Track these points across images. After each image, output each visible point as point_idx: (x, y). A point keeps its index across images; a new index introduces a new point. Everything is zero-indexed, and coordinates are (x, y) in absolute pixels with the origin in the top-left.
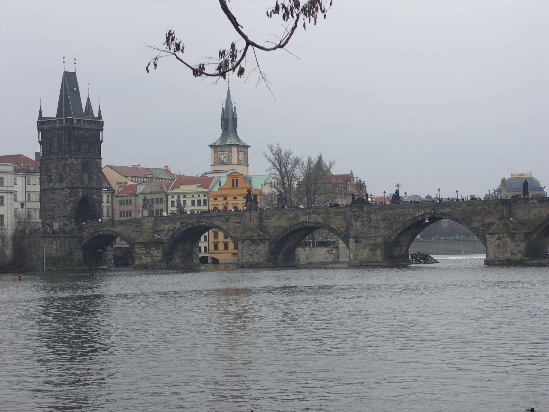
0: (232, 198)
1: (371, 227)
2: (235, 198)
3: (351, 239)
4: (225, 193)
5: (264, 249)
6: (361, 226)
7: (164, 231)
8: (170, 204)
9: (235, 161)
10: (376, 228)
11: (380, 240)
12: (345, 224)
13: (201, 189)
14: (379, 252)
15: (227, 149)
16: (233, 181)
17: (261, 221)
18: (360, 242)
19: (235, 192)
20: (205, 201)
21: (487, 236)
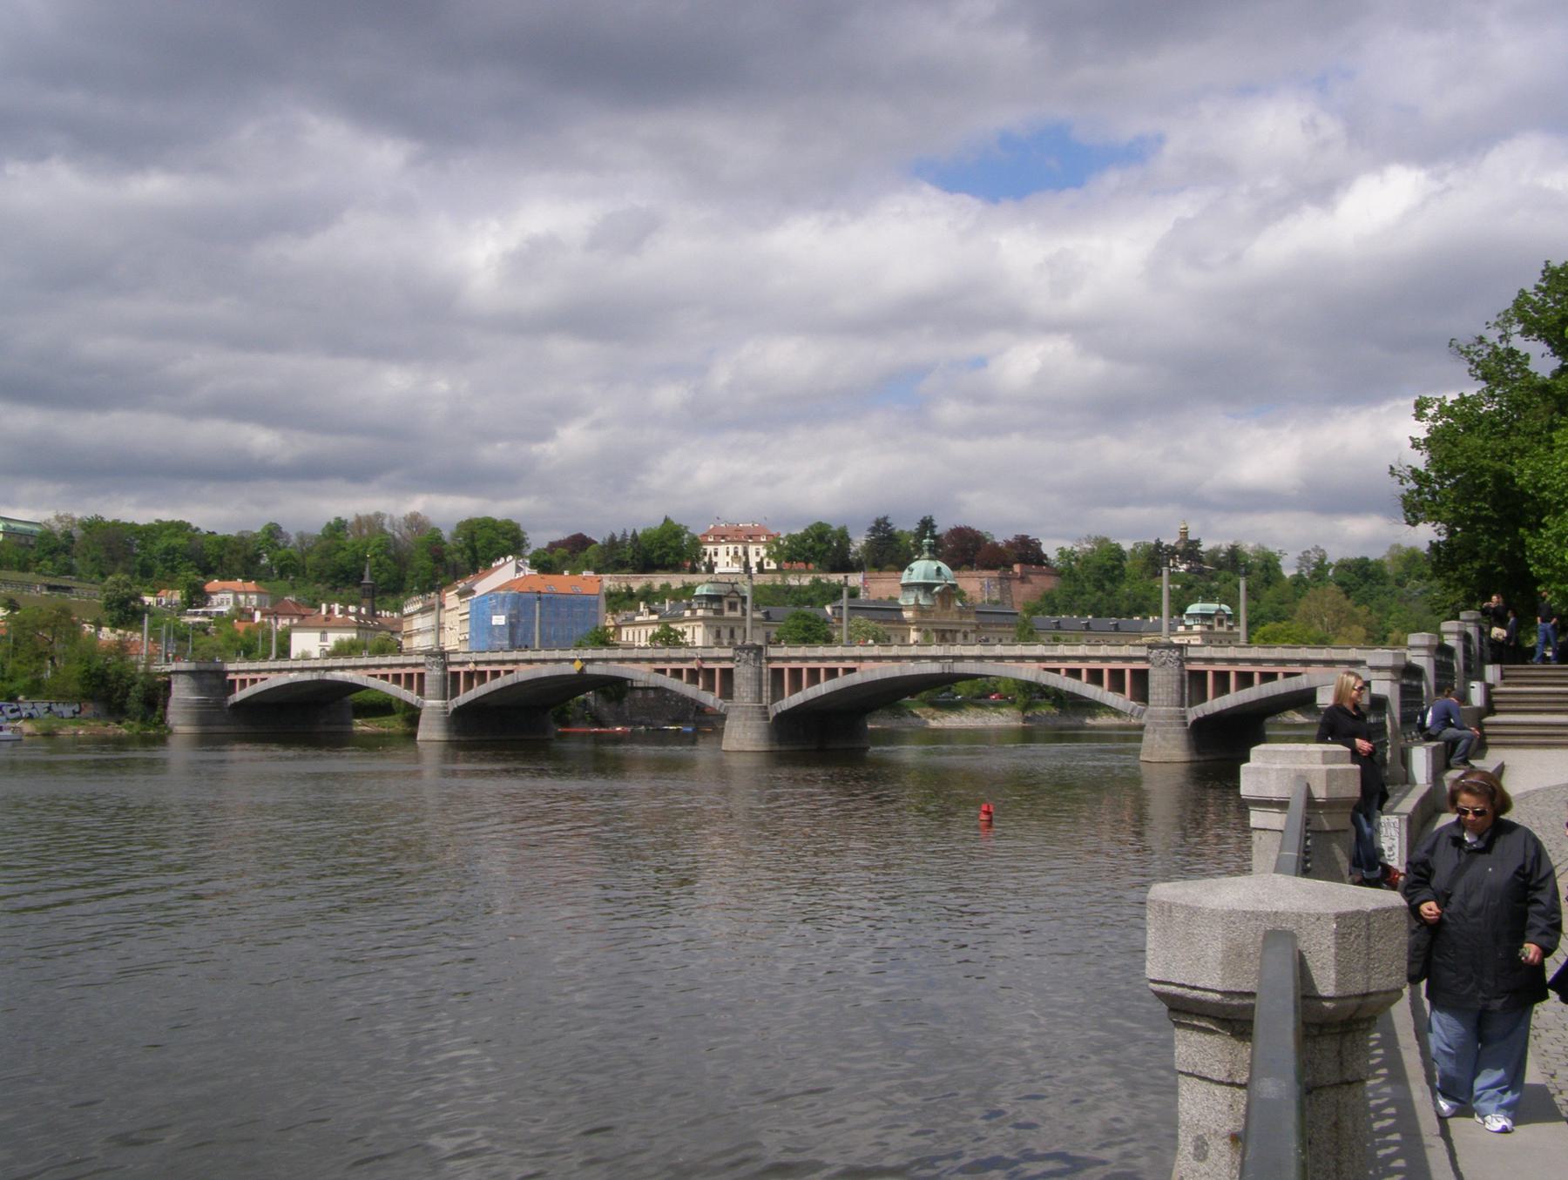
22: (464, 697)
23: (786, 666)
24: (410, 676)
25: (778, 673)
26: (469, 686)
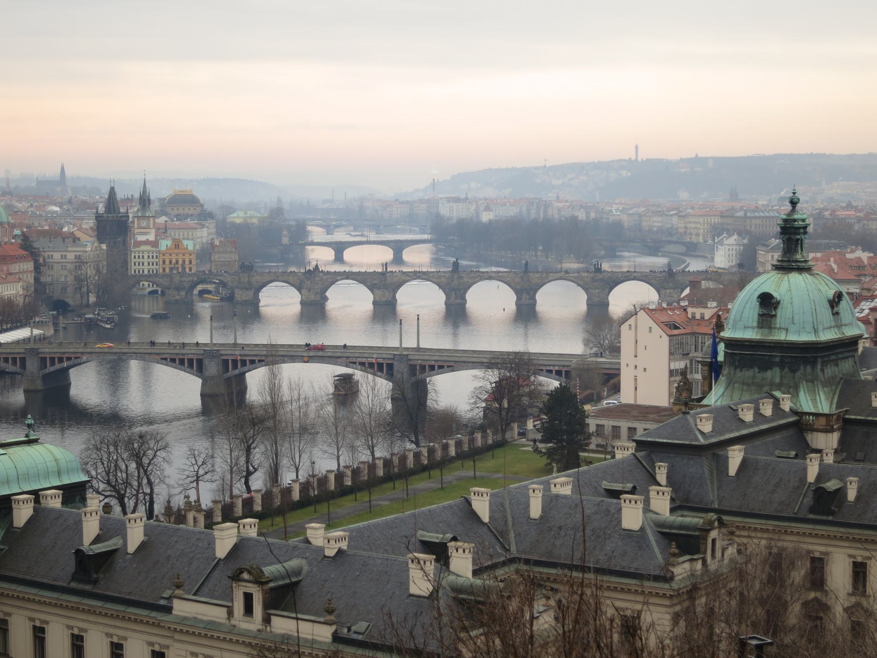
0: (175, 255)
2: (170, 255)
4: (171, 251)
5: (251, 293)
8: (133, 257)
9: (152, 227)
10: (318, 284)
12: (298, 281)
13: (154, 249)
14: (318, 296)
15: (146, 219)
16: (176, 245)
19: (177, 251)
20: (157, 257)
21: (374, 289)
22: (50, 369)
23: (230, 358)
24: (14, 360)
25: (226, 362)
26: (53, 363)
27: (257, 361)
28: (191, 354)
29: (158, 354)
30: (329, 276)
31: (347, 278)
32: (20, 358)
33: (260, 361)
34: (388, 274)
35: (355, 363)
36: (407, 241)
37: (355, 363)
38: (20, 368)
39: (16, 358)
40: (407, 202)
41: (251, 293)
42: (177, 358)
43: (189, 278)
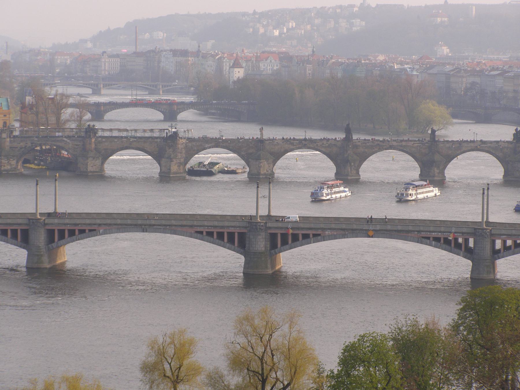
1: (179, 153)
3: (163, 159)
6: (173, 152)
7: (17, 148)
10: (181, 153)
11: (182, 160)
14: (182, 167)
17: (96, 145)
18: (173, 161)
23: (279, 232)
27: (311, 236)
28: (232, 227)
29: (191, 226)
30: (194, 143)
31: (217, 146)
32: (21, 230)
33: (315, 235)
34: (267, 142)
35: (428, 238)
36: (105, 104)
37: (428, 238)
38: (21, 241)
39: (16, 230)
40: (117, 56)
41: (98, 162)
42: (215, 231)
43: (21, 144)
